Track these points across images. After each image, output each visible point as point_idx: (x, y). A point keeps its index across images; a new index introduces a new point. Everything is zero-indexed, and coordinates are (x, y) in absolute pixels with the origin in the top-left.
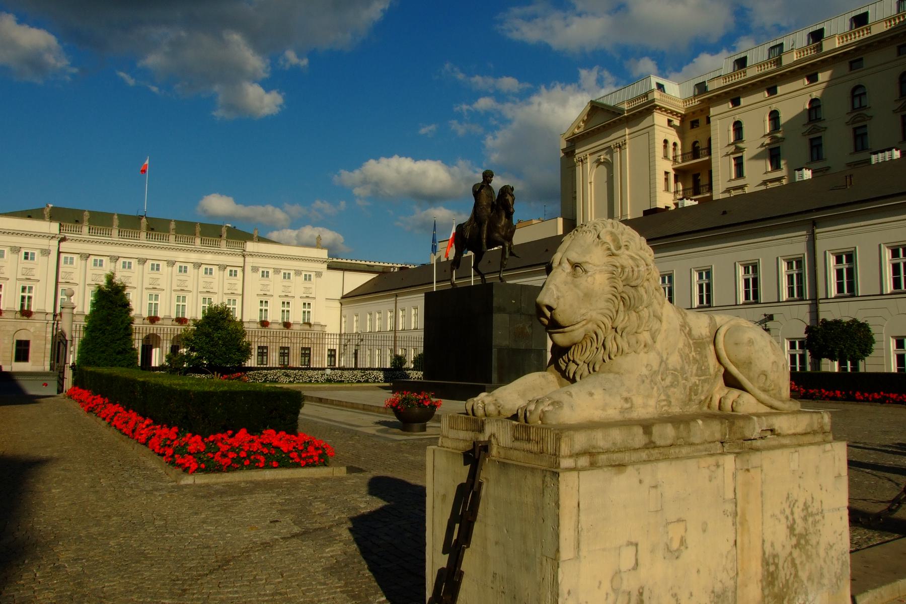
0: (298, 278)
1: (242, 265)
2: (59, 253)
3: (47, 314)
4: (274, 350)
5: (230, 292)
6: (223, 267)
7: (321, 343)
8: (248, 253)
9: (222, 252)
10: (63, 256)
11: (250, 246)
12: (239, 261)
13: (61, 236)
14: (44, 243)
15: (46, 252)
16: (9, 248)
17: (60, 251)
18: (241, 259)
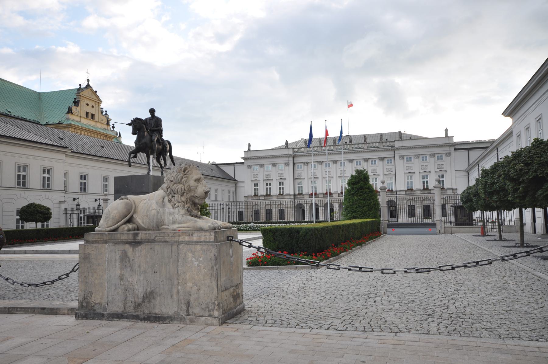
0: (432, 159)
1: (394, 156)
2: (294, 164)
3: (290, 195)
4: (420, 208)
5: (388, 173)
6: (382, 159)
7: (288, 205)
8: (396, 148)
9: (380, 150)
10: (296, 165)
12: (390, 154)
13: (293, 155)
14: (286, 160)
15: (287, 164)
16: (271, 165)
17: (295, 162)
18: (392, 153)
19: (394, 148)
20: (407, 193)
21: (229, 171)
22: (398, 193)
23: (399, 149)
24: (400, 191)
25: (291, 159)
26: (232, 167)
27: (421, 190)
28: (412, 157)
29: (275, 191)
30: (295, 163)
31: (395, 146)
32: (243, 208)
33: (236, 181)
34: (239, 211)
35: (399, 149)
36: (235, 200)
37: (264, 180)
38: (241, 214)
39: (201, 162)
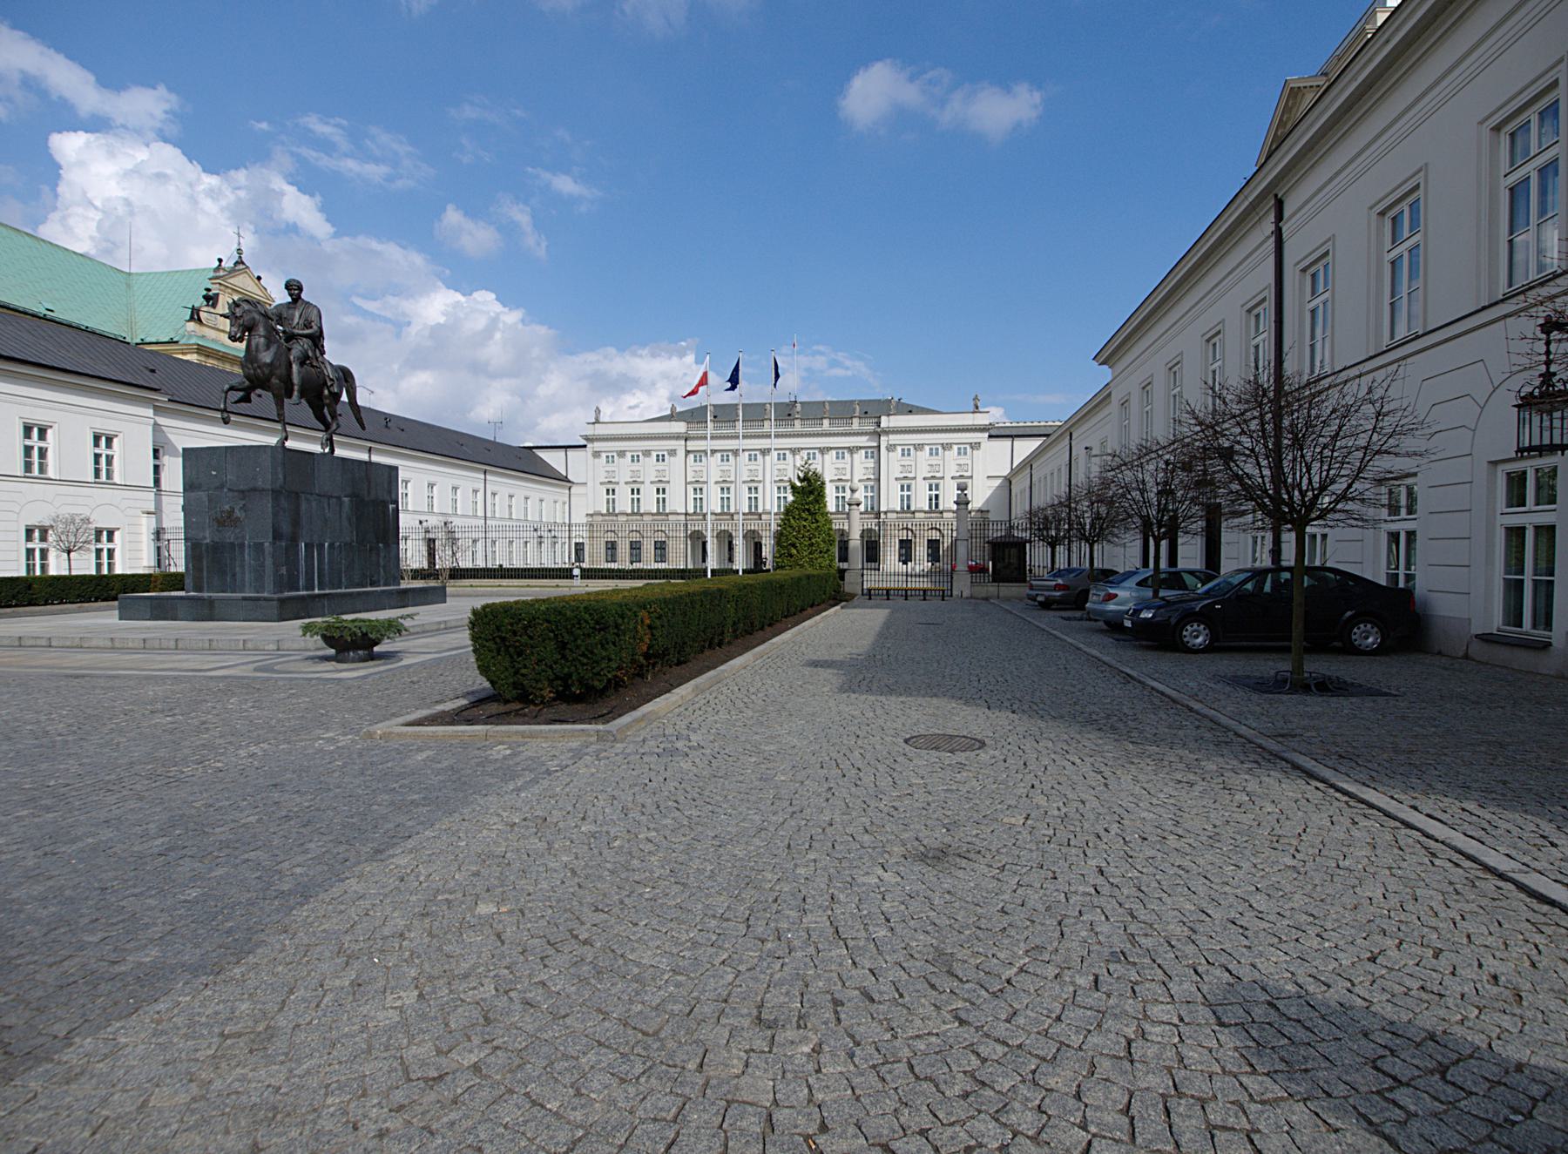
1: (875, 444)
2: (688, 452)
3: (678, 514)
11: (885, 422)
15: (673, 453)
17: (688, 449)
19: (879, 430)
20: (900, 515)
21: (553, 459)
22: (882, 516)
23: (887, 432)
24: (886, 513)
25: (683, 442)
26: (561, 453)
27: (926, 512)
28: (912, 448)
29: (649, 504)
30: (689, 452)
31: (882, 425)
32: (580, 535)
33: (569, 481)
34: (576, 544)
35: (887, 432)
36: (567, 522)
37: (626, 483)
38: (579, 548)
39: (497, 440)
